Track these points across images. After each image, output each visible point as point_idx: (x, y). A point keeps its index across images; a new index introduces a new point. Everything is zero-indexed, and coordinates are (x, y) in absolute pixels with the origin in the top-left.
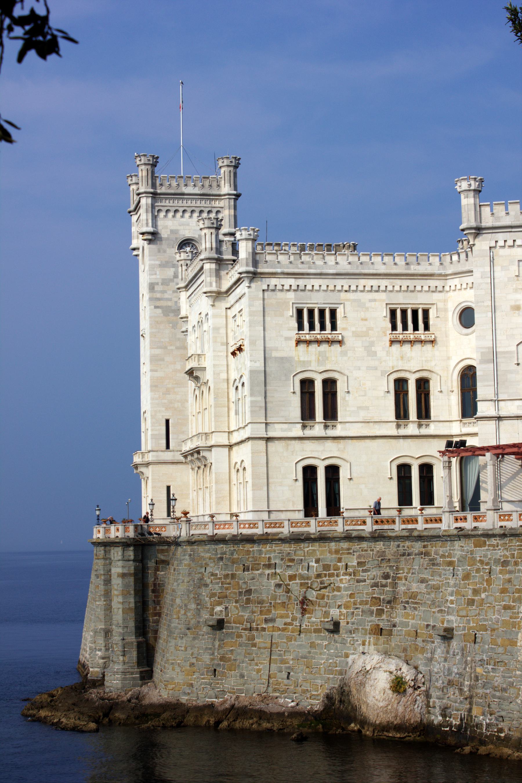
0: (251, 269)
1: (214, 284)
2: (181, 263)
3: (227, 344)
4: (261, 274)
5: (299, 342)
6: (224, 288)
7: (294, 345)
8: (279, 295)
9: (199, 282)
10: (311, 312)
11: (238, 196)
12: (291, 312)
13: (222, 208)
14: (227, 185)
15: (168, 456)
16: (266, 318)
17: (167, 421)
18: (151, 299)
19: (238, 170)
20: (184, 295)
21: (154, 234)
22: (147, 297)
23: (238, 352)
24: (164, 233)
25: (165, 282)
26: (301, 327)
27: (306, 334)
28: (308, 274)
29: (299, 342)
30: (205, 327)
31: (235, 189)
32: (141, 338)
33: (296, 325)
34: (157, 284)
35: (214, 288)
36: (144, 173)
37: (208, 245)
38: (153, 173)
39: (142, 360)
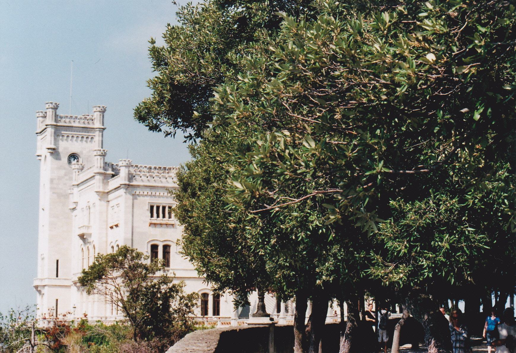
0: (127, 183)
1: (101, 187)
2: (75, 170)
3: (107, 221)
4: (132, 185)
5: (151, 224)
6: (107, 191)
7: (149, 225)
8: (141, 198)
9: (88, 184)
10: (158, 207)
11: (104, 129)
12: (148, 207)
13: (94, 136)
14: (98, 122)
15: (57, 282)
16: (135, 210)
17: (57, 261)
18: (51, 188)
19: (105, 114)
20: (76, 189)
21: (54, 149)
22: (48, 186)
23: (114, 227)
24: (60, 150)
25: (60, 178)
26: (152, 216)
27: (155, 220)
28: (158, 187)
29: (151, 224)
30: (92, 210)
31: (103, 125)
32: (41, 210)
33: (150, 214)
34: (55, 179)
35: (101, 190)
36: (51, 113)
37: (99, 165)
38: (56, 113)
39: (41, 223)
